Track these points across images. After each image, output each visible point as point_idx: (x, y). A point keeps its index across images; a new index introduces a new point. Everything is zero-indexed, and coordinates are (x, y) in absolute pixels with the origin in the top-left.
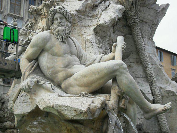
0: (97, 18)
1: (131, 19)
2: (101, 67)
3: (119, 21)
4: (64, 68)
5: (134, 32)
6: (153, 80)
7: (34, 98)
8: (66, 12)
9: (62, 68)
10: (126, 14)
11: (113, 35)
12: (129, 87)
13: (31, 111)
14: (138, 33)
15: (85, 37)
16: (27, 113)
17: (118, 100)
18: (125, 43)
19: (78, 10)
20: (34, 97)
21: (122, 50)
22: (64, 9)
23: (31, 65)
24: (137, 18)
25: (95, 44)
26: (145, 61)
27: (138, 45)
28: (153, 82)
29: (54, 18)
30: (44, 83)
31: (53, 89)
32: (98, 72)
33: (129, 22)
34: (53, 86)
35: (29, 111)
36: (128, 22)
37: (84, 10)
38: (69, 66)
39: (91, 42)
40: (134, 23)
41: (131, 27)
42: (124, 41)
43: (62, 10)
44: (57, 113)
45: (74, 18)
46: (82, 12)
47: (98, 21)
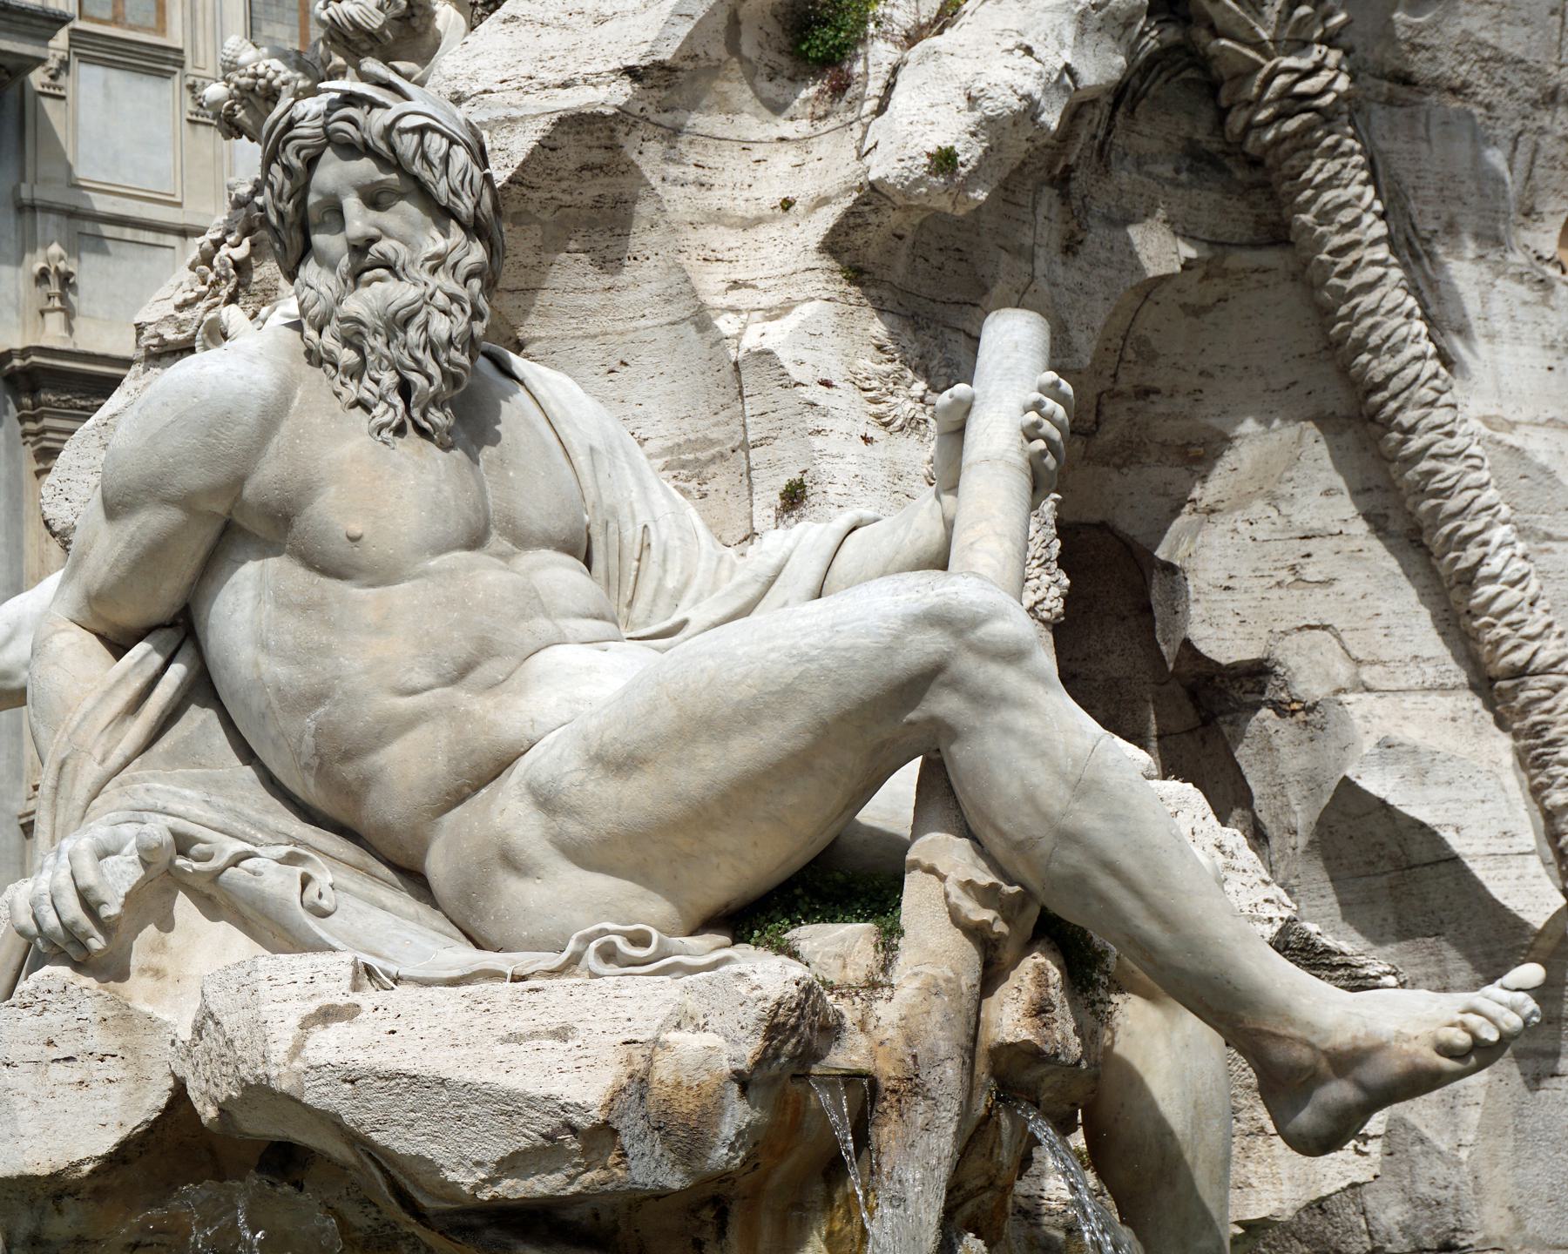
0: (850, 116)
1: (1261, 75)
2: (773, 656)
3: (1132, 111)
4: (430, 688)
5: (1307, 218)
6: (1547, 705)
7: (147, 1009)
8: (421, 130)
9: (414, 692)
10: (1202, 35)
11: (1060, 270)
12: (1070, 837)
13: (124, 1145)
14: (1346, 216)
15: (738, 337)
16: (90, 1159)
17: (970, 978)
18: (1052, 376)
19: (643, 63)
20: (141, 1006)
21: (1020, 460)
22: (398, 106)
23: (122, 680)
24: (1318, 68)
25: (844, 399)
26: (1452, 505)
27: (1361, 346)
28: (1552, 734)
29: (313, 199)
30: (236, 861)
31: (324, 914)
32: (749, 715)
33: (1244, 115)
34: (324, 877)
35: (106, 1143)
36: (1230, 118)
37: (718, 51)
38: (489, 670)
39: (796, 374)
40: (1291, 125)
41: (1269, 161)
42: (1041, 360)
43: (377, 112)
44: (338, 1150)
45: (613, 148)
46: (693, 79)
47: (860, 157)
